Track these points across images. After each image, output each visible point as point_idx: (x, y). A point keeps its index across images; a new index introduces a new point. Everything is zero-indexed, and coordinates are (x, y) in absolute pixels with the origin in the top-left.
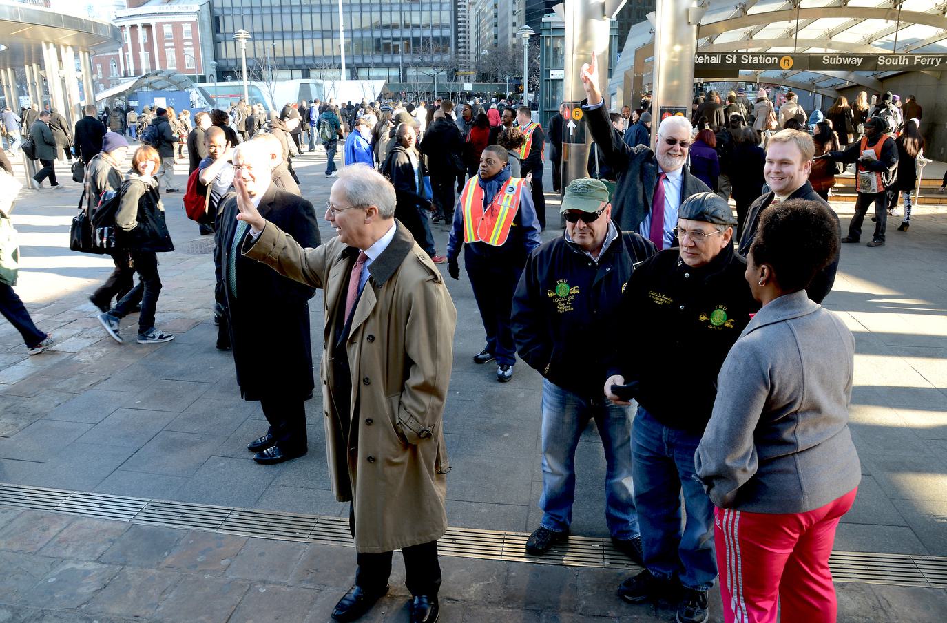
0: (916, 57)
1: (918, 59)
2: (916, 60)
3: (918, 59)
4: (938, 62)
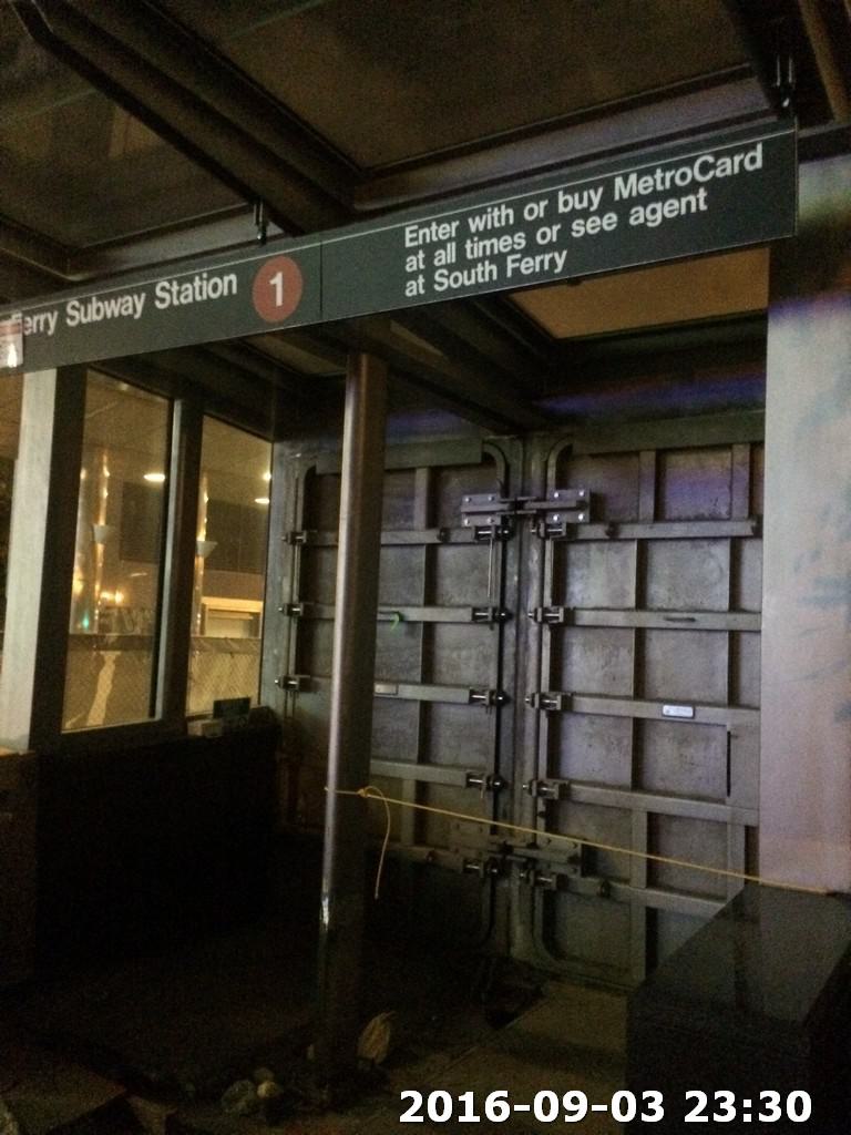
4: (52, 324)
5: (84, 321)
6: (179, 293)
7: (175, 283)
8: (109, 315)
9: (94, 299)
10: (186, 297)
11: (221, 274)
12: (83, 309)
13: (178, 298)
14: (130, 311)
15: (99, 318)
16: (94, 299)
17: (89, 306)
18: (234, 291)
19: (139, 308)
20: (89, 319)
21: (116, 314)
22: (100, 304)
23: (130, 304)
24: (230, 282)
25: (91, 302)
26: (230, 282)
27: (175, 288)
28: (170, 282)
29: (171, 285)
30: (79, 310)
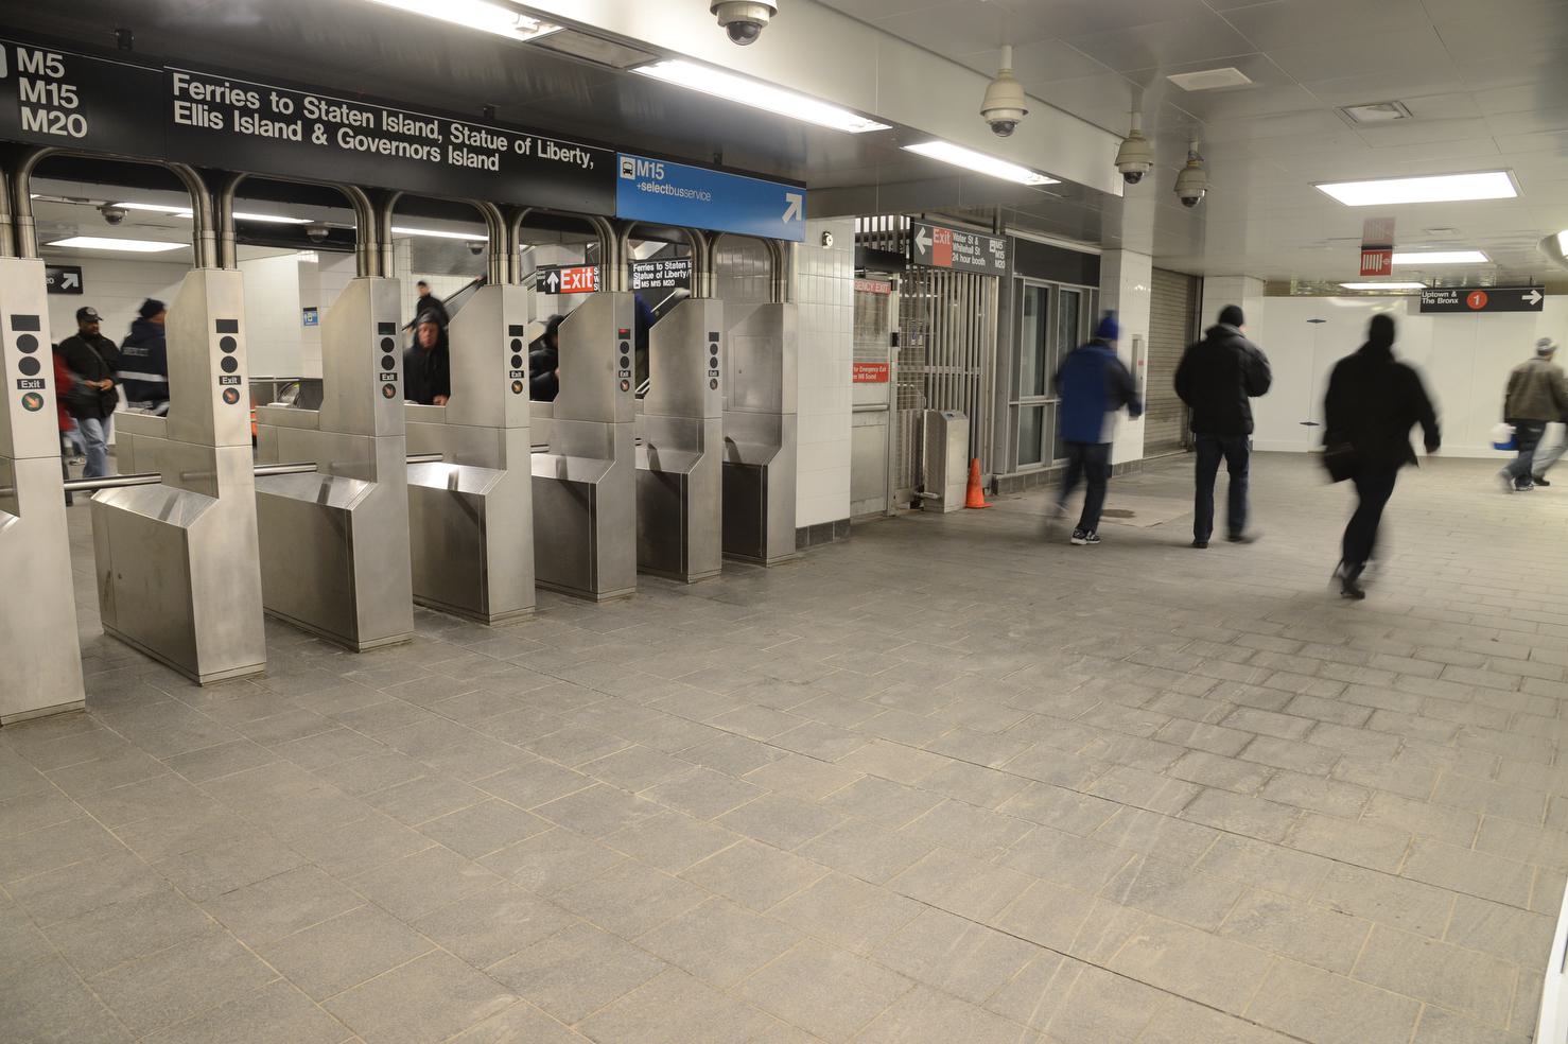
0: (176, 76)
1: (181, 80)
2: (177, 85)
3: (181, 80)
6: (327, 112)
7: (323, 103)
10: (335, 117)
11: (362, 110)
13: (327, 116)
18: (372, 126)
24: (368, 119)
26: (368, 119)
27: (323, 106)
28: (319, 100)
29: (320, 103)
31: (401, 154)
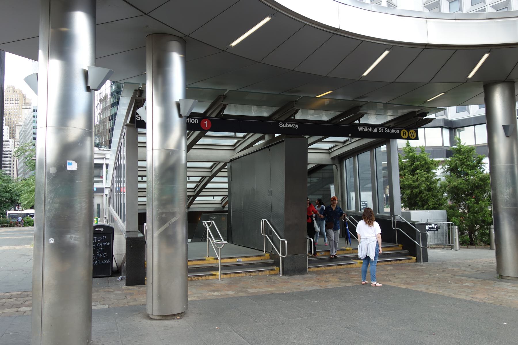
5: (284, 127)
8: (290, 127)
9: (286, 123)
12: (283, 124)
14: (295, 127)
15: (288, 127)
16: (286, 123)
17: (285, 124)
19: (297, 127)
20: (285, 126)
21: (292, 127)
22: (287, 124)
23: (295, 126)
25: (285, 124)
30: (282, 124)
31: (363, 131)
